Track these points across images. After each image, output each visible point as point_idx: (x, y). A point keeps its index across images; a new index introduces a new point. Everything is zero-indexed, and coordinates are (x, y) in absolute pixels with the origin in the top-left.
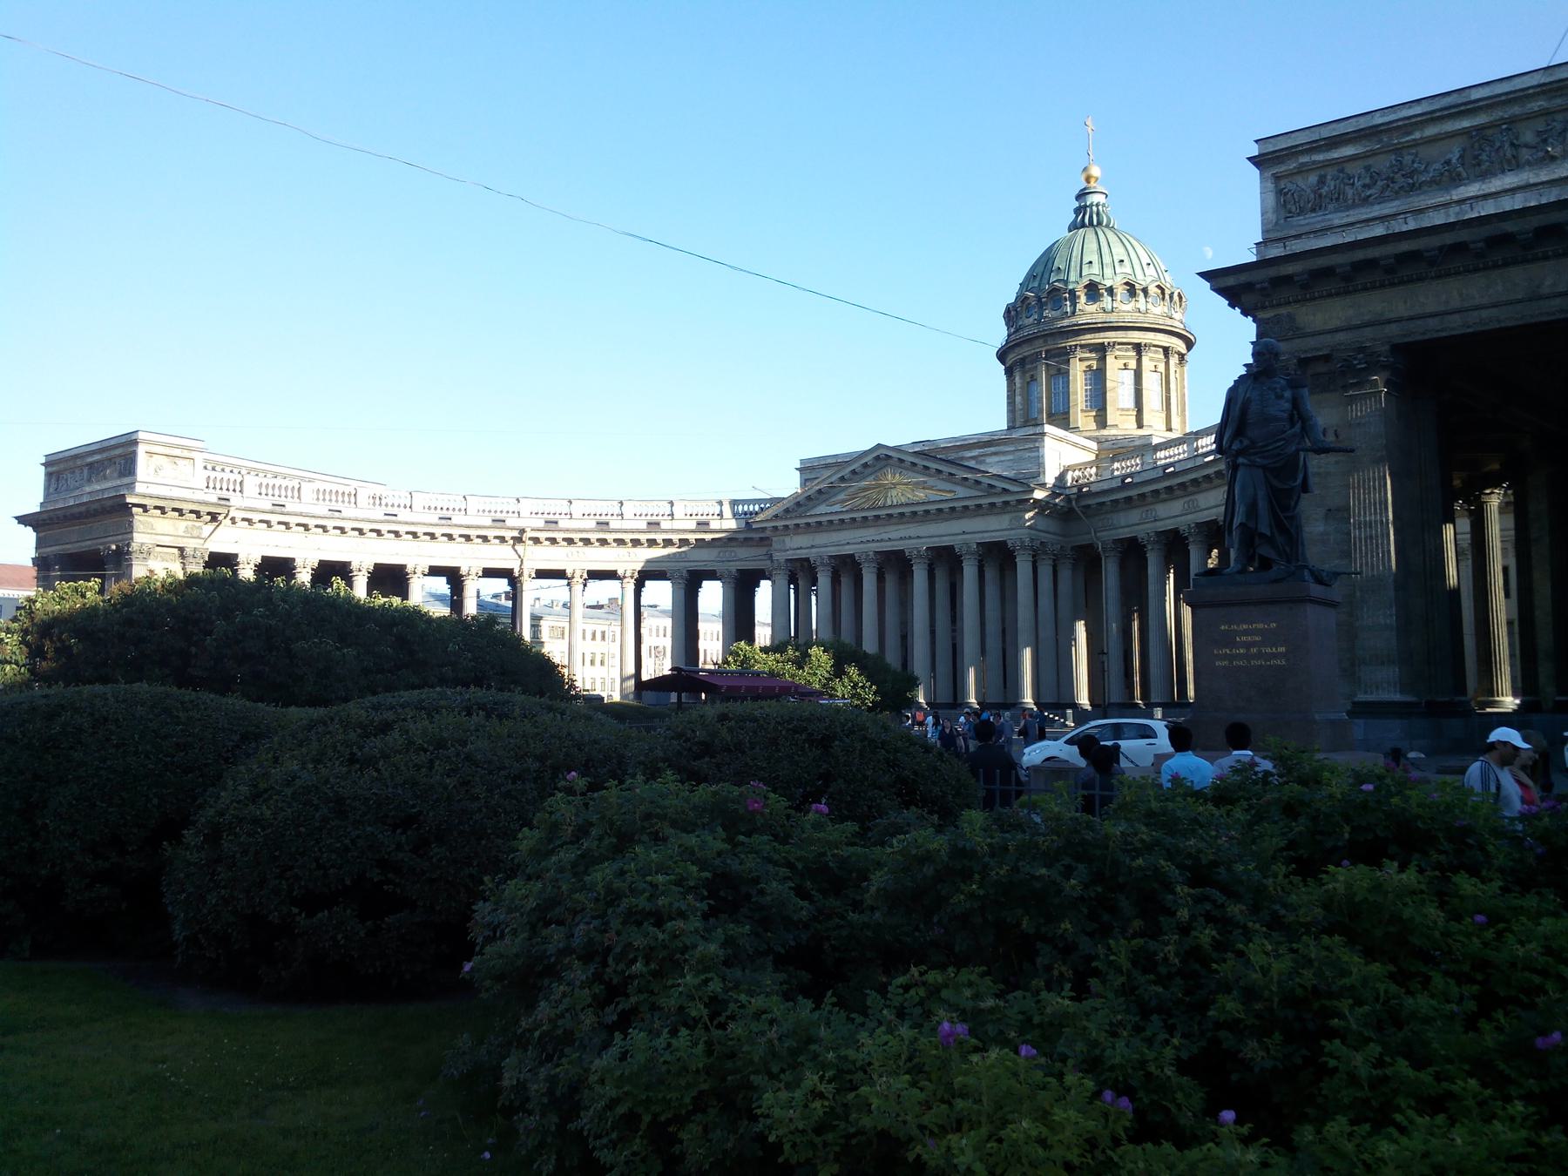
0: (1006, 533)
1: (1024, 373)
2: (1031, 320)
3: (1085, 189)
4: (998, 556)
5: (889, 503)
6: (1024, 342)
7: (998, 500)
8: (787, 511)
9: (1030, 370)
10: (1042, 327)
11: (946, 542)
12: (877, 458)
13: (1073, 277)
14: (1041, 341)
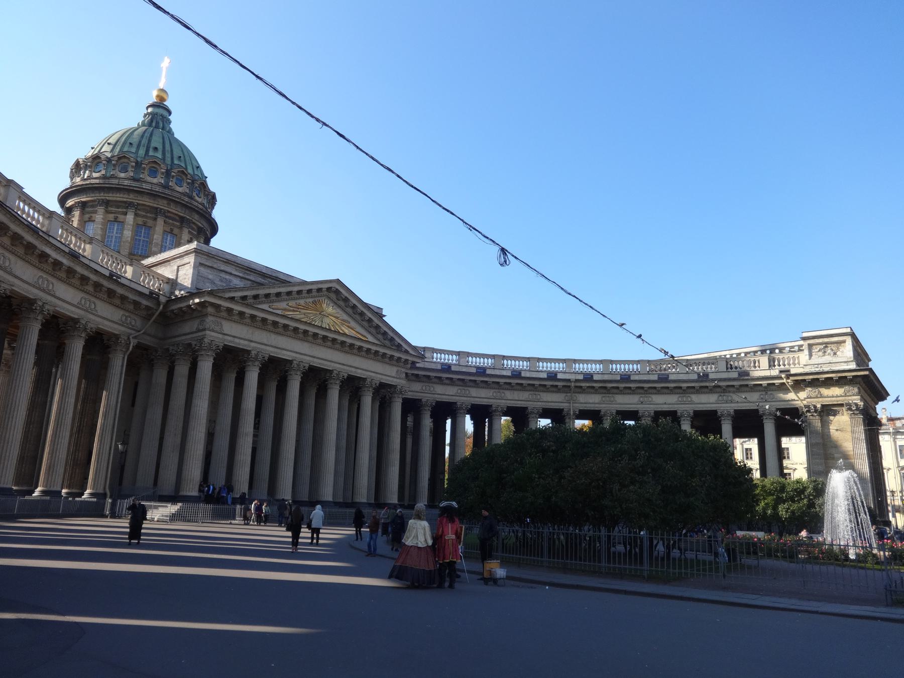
0: (395, 380)
1: (136, 215)
2: (155, 181)
3: (156, 102)
4: (383, 394)
5: (324, 326)
6: (148, 193)
7: (404, 357)
8: (244, 298)
9: (143, 216)
10: (167, 191)
11: (359, 373)
12: (329, 289)
13: (190, 171)
14: (165, 202)
